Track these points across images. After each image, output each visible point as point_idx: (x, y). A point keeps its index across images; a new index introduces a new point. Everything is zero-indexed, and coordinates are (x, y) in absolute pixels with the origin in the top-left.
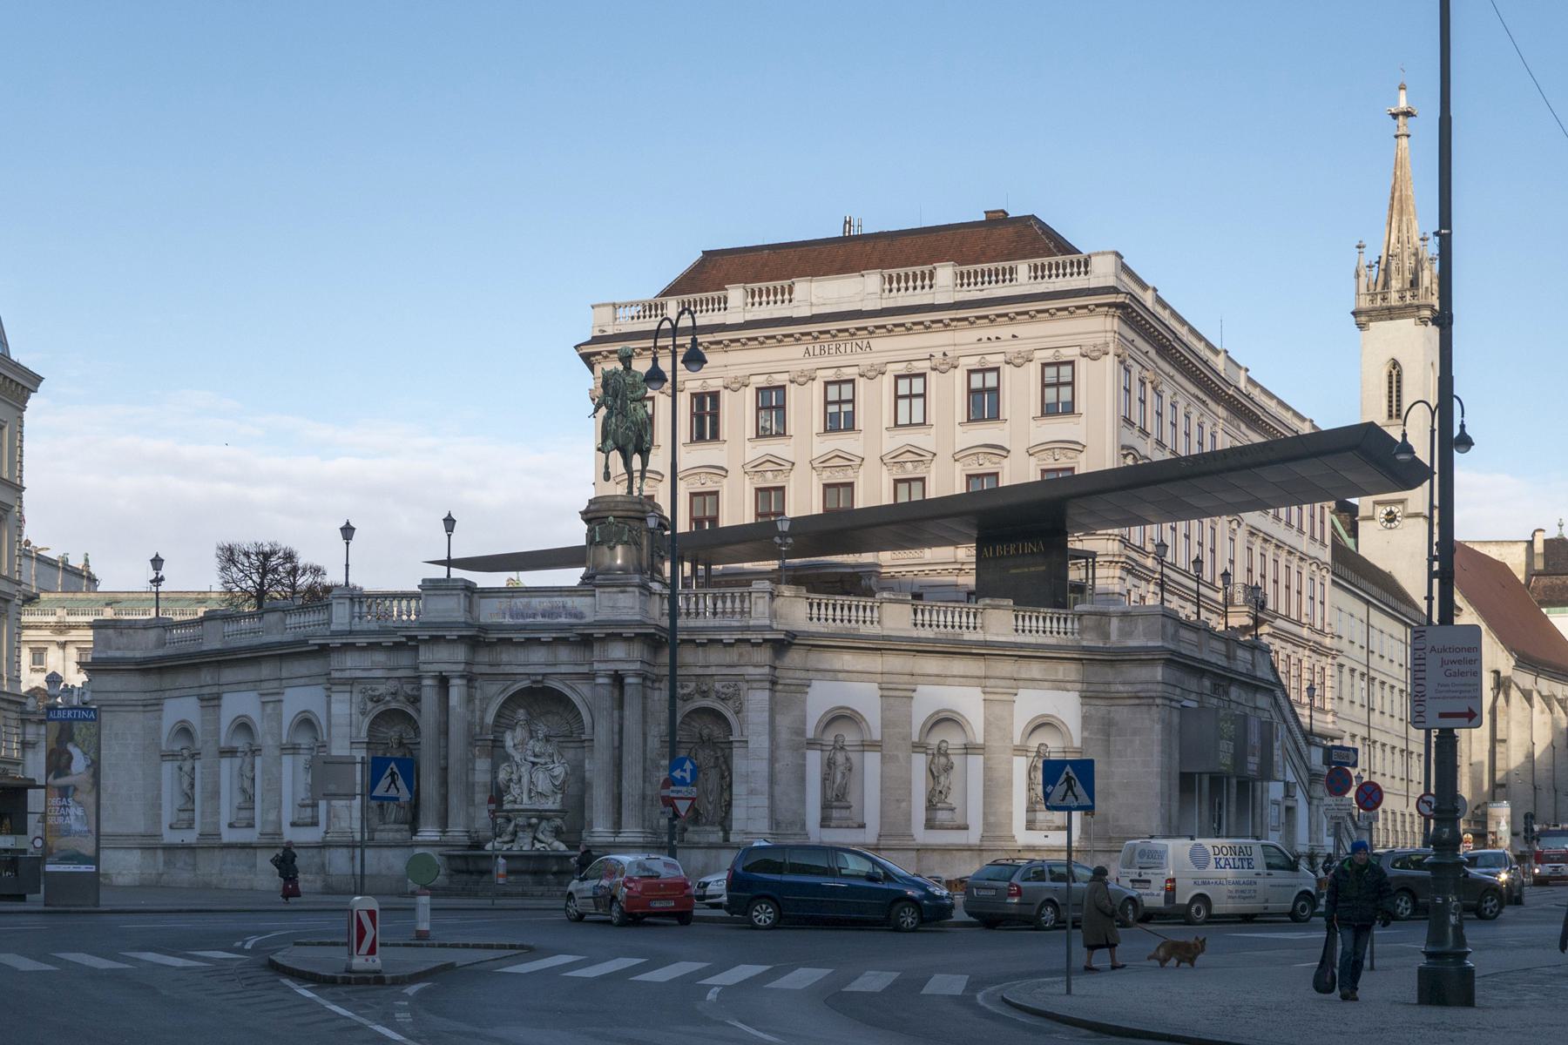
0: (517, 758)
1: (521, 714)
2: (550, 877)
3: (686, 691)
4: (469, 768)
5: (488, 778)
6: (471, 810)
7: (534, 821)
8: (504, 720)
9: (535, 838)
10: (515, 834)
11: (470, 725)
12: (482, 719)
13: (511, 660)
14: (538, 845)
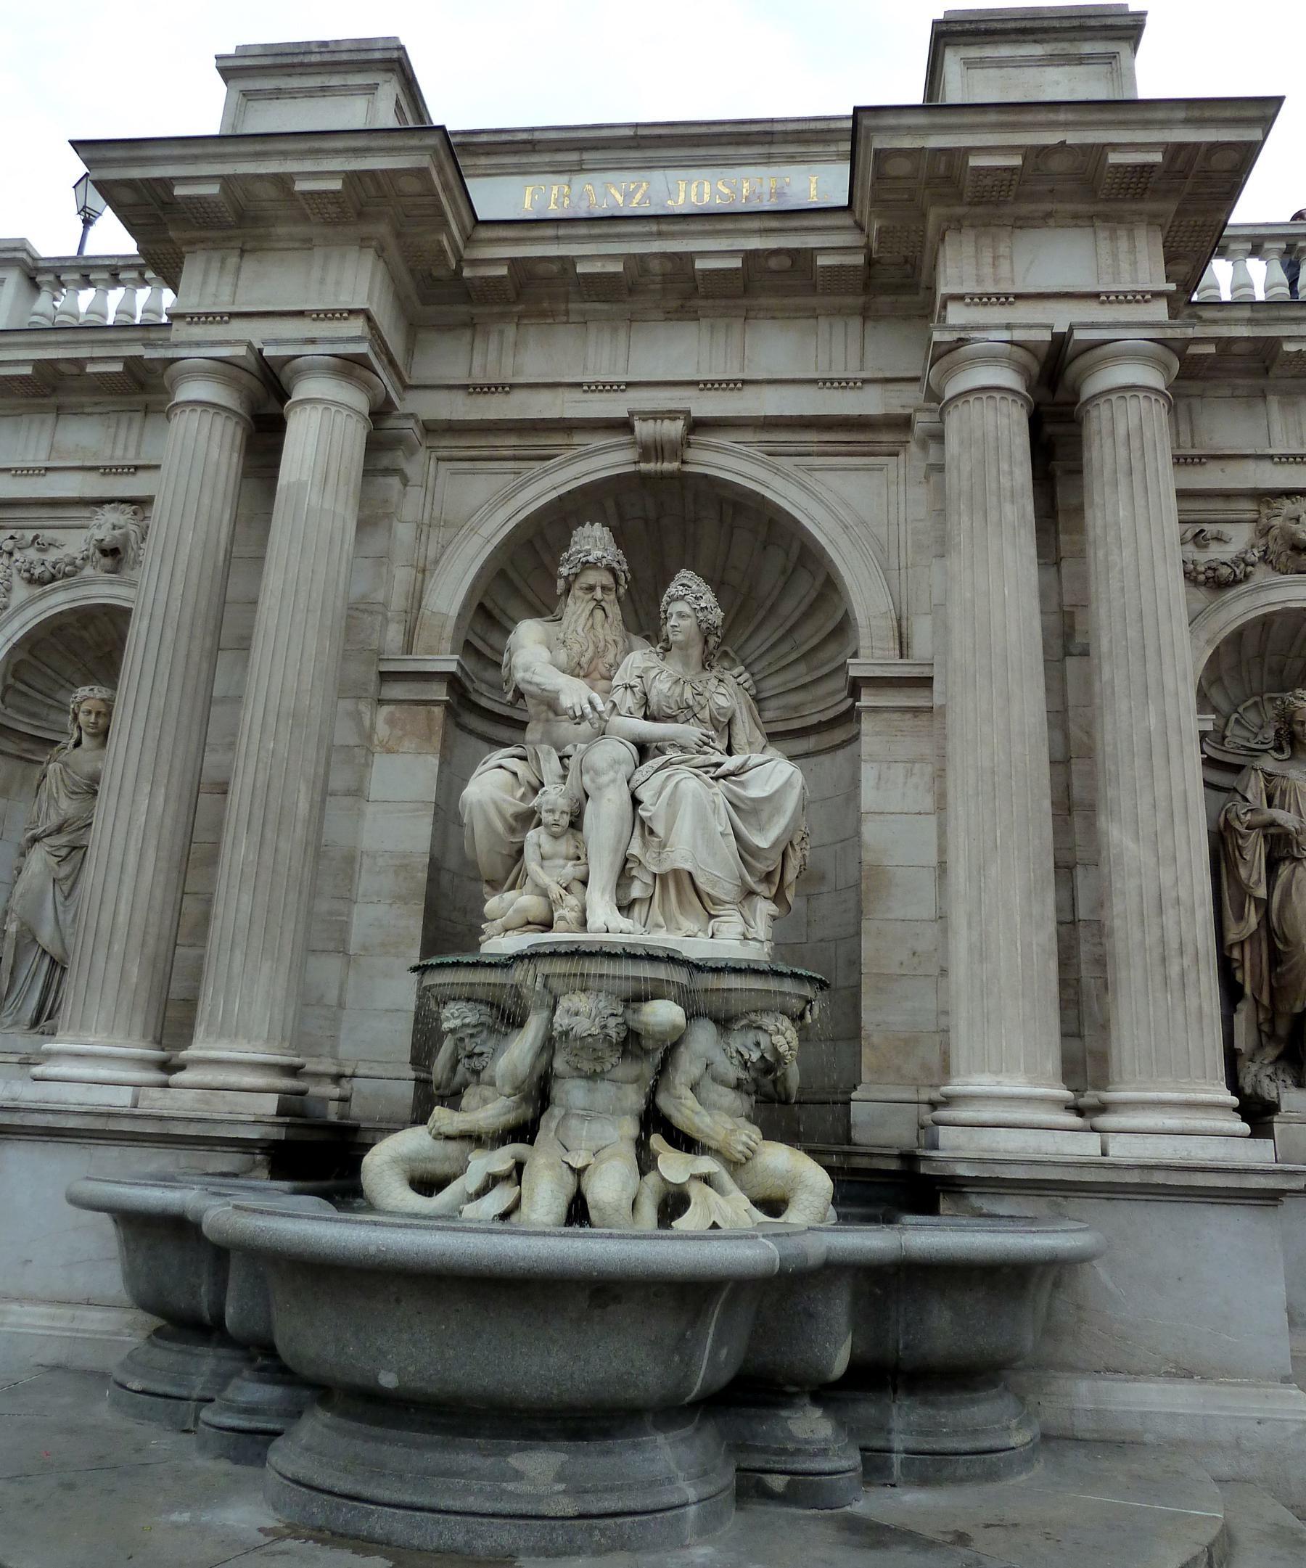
0: (574, 693)
1: (593, 541)
2: (810, 1423)
3: (1217, 553)
4: (339, 778)
5: (417, 836)
6: (327, 970)
7: (664, 1013)
8: (523, 576)
9: (654, 1121)
10: (539, 1092)
11: (356, 615)
12: (417, 597)
13: (562, 368)
14: (675, 1166)
